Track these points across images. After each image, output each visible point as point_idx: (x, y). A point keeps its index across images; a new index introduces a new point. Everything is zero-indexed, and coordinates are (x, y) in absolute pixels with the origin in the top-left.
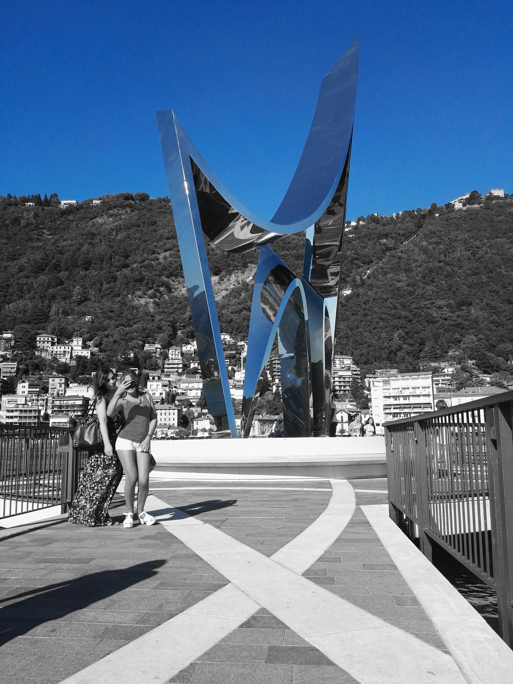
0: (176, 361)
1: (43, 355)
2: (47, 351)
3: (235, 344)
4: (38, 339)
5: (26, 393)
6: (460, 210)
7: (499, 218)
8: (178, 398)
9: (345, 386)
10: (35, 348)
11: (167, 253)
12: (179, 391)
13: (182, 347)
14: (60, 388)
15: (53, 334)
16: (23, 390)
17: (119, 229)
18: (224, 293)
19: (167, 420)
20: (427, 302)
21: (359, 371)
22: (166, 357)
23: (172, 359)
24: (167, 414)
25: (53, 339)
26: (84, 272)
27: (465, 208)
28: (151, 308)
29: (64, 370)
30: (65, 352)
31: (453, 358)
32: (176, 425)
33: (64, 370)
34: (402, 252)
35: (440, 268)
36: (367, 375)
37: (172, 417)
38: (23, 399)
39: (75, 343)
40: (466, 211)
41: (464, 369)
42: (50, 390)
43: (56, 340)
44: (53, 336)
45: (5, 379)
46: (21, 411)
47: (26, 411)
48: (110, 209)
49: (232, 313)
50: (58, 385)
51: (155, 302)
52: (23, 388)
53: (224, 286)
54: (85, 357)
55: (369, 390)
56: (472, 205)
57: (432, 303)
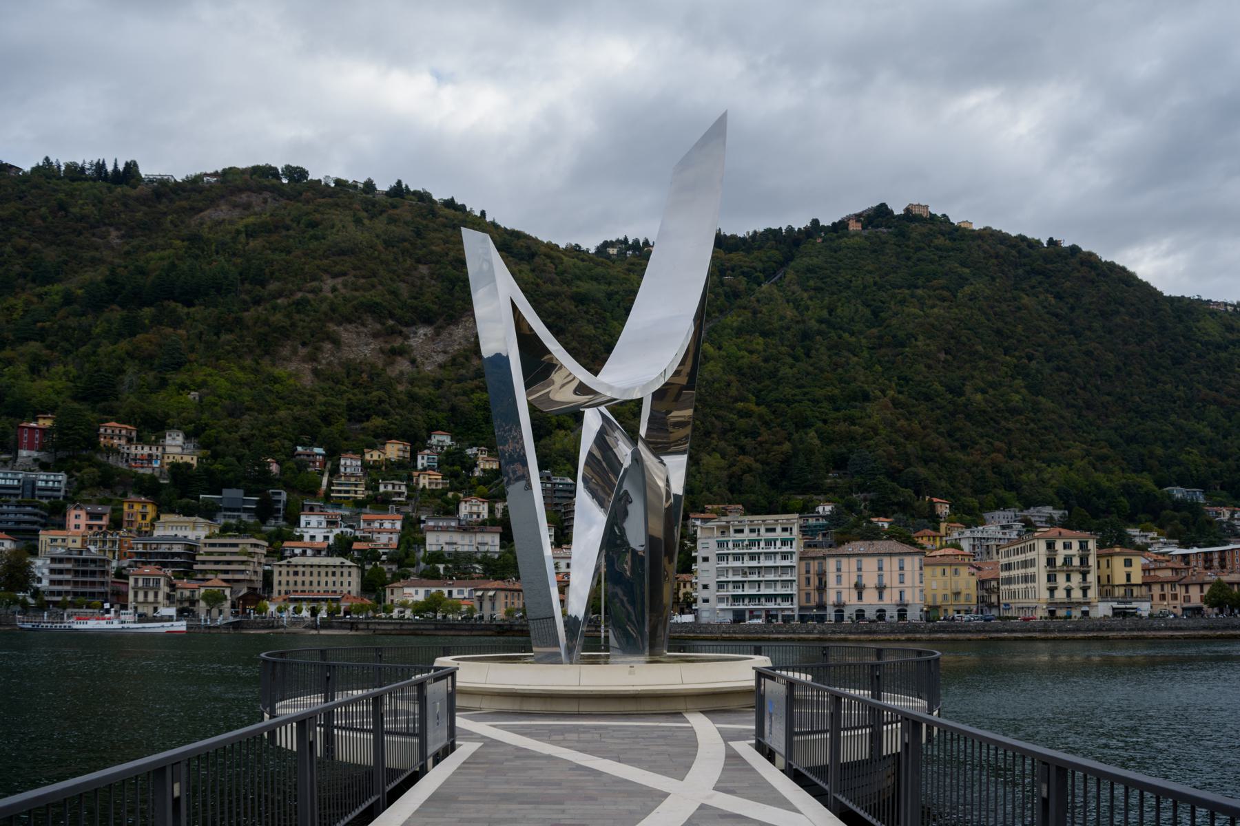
0: (353, 480)
1: (112, 460)
2: (118, 452)
3: (461, 452)
4: (102, 430)
5: (83, 528)
6: (857, 234)
7: (919, 254)
8: (356, 546)
11: (340, 280)
12: (358, 534)
13: (363, 454)
15: (129, 423)
16: (77, 522)
17: (251, 233)
18: (440, 358)
19: (338, 584)
20: (797, 391)
22: (335, 472)
23: (345, 475)
24: (338, 574)
26: (186, 310)
27: (865, 233)
28: (307, 380)
29: (148, 488)
30: (150, 455)
31: (832, 489)
32: (354, 593)
33: (148, 488)
34: (758, 301)
35: (820, 333)
36: (691, 515)
37: (346, 579)
38: (79, 540)
39: (168, 440)
40: (867, 238)
41: (851, 507)
42: (125, 524)
43: (134, 434)
45: (45, 501)
46: (76, 560)
47: (85, 561)
48: (232, 193)
49: (456, 395)
50: (140, 517)
51: (316, 372)
52: (77, 519)
53: (441, 345)
55: (694, 541)
56: (877, 227)
57: (805, 394)
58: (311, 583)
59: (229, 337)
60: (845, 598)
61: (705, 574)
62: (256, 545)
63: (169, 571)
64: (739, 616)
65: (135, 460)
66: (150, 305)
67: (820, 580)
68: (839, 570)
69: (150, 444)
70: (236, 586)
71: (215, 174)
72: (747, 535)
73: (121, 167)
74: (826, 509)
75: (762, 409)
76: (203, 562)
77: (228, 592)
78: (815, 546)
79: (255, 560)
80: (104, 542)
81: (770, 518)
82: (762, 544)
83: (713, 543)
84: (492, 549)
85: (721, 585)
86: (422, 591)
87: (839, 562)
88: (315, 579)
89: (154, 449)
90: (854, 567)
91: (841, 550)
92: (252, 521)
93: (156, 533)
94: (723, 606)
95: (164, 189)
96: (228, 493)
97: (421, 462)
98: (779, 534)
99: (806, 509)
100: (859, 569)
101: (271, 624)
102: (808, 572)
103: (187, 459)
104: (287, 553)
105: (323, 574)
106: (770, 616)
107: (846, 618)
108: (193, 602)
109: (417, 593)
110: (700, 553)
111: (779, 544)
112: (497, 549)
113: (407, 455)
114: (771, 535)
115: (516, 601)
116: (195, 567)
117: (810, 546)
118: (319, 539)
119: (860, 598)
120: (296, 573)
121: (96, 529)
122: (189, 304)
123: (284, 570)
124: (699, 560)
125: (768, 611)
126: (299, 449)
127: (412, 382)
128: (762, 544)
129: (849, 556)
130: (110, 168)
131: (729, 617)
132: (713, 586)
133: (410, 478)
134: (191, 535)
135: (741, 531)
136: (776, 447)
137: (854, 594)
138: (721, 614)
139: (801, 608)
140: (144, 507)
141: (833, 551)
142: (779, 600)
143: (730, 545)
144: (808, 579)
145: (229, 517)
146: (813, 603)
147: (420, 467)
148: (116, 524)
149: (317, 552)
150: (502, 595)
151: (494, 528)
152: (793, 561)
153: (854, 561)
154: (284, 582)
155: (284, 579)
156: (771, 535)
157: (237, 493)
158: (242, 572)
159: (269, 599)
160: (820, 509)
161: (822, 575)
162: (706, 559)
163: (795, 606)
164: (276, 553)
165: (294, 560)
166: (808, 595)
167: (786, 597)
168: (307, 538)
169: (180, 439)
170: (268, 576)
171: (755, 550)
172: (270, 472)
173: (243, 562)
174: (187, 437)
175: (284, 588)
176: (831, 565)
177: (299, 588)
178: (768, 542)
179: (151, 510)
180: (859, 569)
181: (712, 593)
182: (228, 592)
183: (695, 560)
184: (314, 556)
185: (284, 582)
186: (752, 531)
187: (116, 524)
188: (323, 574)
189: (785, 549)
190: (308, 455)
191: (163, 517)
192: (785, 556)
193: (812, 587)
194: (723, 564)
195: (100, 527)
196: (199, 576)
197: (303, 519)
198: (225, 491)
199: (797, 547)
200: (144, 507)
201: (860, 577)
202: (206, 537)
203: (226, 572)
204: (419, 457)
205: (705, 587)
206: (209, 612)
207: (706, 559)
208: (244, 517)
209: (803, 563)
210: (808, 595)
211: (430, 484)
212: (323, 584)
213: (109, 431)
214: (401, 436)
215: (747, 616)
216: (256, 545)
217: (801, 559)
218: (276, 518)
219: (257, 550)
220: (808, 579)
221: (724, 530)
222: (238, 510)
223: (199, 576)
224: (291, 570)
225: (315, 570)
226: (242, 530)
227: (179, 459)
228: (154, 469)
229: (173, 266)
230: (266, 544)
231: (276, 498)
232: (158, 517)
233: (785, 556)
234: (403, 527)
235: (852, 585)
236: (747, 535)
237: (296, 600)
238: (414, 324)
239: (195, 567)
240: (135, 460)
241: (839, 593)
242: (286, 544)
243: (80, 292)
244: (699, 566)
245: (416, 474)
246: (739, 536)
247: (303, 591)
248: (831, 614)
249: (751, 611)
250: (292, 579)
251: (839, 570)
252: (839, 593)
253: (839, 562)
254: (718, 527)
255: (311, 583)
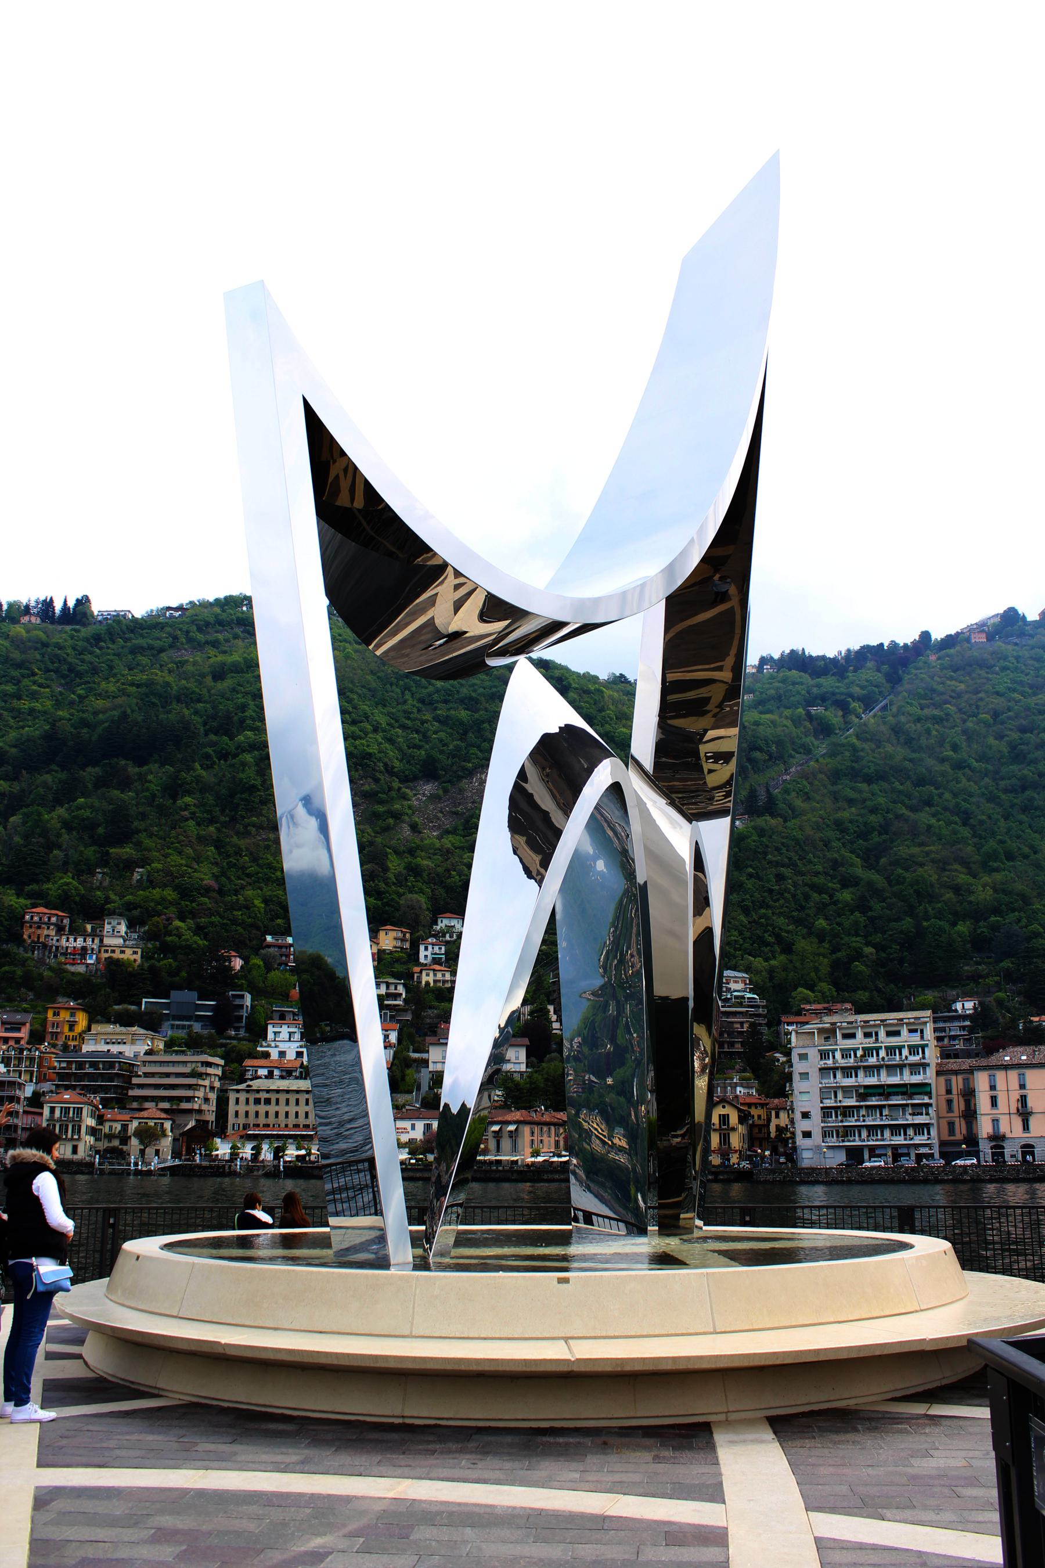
4: (27, 917)
9: (732, 1044)
10: (19, 940)
14: (71, 1034)
21: (763, 1007)
25: (61, 919)
26: (137, 770)
30: (84, 949)
31: (975, 978)
36: (783, 1019)
42: (48, 1037)
43: (66, 921)
44: (60, 914)
50: (66, 1028)
54: (128, 963)
55: (788, 1053)
58: (277, 1114)
59: (188, 799)
60: (1004, 1128)
61: (805, 1097)
62: (209, 1064)
63: (96, 1099)
64: (855, 1155)
65: (65, 954)
66: (95, 764)
67: (968, 1103)
68: (993, 1088)
69: (85, 935)
70: (180, 1119)
71: (180, 608)
72: (860, 1041)
73: (71, 604)
74: (966, 1006)
75: (875, 877)
76: (141, 1086)
77: (168, 1125)
78: (956, 1056)
79: (207, 1083)
80: (20, 1060)
81: (892, 1017)
82: (882, 1053)
83: (813, 1053)
84: (516, 1068)
85: (826, 1112)
86: (420, 1125)
87: (992, 1078)
88: (282, 1109)
89: (89, 940)
90: (1014, 1084)
91: (993, 1060)
92: (206, 1032)
93: (86, 1048)
94: (833, 1141)
95: (122, 628)
96: (177, 996)
97: (425, 954)
98: (906, 1038)
99: (942, 1012)
100: (1022, 1086)
101: (221, 1170)
102: (949, 1092)
103: (128, 955)
104: (249, 1075)
105: (293, 1101)
106: (897, 1153)
107: (1007, 1158)
108: (125, 1140)
109: (413, 1127)
110: (798, 1067)
111: (905, 1052)
112: (523, 1068)
113: (407, 945)
114: (894, 1041)
115: (545, 1138)
116: (131, 1093)
117: (948, 1056)
118: (291, 1055)
119: (1026, 1127)
120: (257, 1101)
121: (12, 1043)
122: (141, 762)
123: (242, 1097)
124: (796, 1077)
125: (895, 1148)
126: (269, 938)
127: (412, 852)
128: (882, 1053)
129: (1006, 1067)
130: (58, 606)
131: (841, 1157)
132: (816, 1114)
133: (411, 975)
134: (129, 1050)
135: (853, 1036)
136: (893, 924)
137: (1018, 1122)
138: (830, 1154)
139: (942, 1144)
140: (73, 1015)
141: (984, 1062)
142: (910, 1132)
143: (838, 1055)
144: (949, 1102)
145: (178, 1027)
146: (958, 1137)
147: (422, 960)
148: (37, 1037)
149: (287, 1074)
150: (526, 1130)
151: (519, 1040)
152: (929, 1076)
153: (1013, 1075)
154: (242, 1114)
155: (242, 1108)
156: (894, 1041)
157: (189, 996)
158: (189, 1099)
159: (222, 1133)
160: (959, 1006)
161: (969, 1094)
162: (805, 1076)
163: (935, 1141)
164: (235, 1075)
165: (256, 1084)
166: (951, 1125)
167: (919, 1128)
168: (274, 1055)
169: (123, 928)
170: (222, 1103)
171: (872, 1060)
172: (231, 969)
173: (189, 1087)
174: (130, 926)
175: (242, 1120)
176: (981, 1081)
177: (262, 1120)
178: (891, 1050)
179: (82, 1020)
180: (1022, 1086)
181: (815, 1124)
182: (168, 1125)
183: (789, 1078)
184: (282, 1077)
185: (242, 1114)
186: (867, 1035)
187: (37, 1037)
188: (293, 1101)
189: (914, 1059)
190: (280, 947)
191: (96, 1028)
192: (915, 1068)
193: (956, 1113)
194: (830, 1081)
195: (18, 1040)
196: (135, 1105)
197: (271, 1030)
198: (173, 993)
199: (932, 1055)
200: (73, 1015)
201: (1023, 1099)
202: (147, 1053)
203: (170, 1099)
204: (422, 948)
205: (806, 1115)
206: (142, 1152)
207: (805, 1076)
208: (197, 1027)
209: (942, 1079)
210: (951, 1125)
211: (435, 981)
212: (292, 1115)
213: (36, 919)
214: (397, 923)
215: (866, 1156)
216: (209, 1064)
217: (939, 1073)
218: (237, 1029)
219: (210, 1070)
220: (949, 1102)
221: (829, 1034)
222: (188, 1018)
223: (135, 1105)
224: (252, 1097)
225: (283, 1097)
226: (194, 1043)
227: (117, 955)
228: (88, 965)
229: (124, 715)
230: (222, 1062)
231: (238, 1002)
232: (89, 1028)
233: (915, 1068)
234: (400, 1040)
235: (1013, 1110)
236: (860, 1041)
237: (254, 1137)
238: (415, 778)
239: (131, 1093)
240: (65, 954)
241: (995, 1122)
242: (248, 1062)
243: (14, 750)
244: (798, 1085)
245: (417, 969)
246: (849, 1043)
247: (267, 1126)
248: (986, 1148)
249: (872, 1149)
250: (252, 1108)
251: (993, 1088)
252: (995, 1122)
253: (992, 1078)
254: (821, 1031)
255: (277, 1114)
